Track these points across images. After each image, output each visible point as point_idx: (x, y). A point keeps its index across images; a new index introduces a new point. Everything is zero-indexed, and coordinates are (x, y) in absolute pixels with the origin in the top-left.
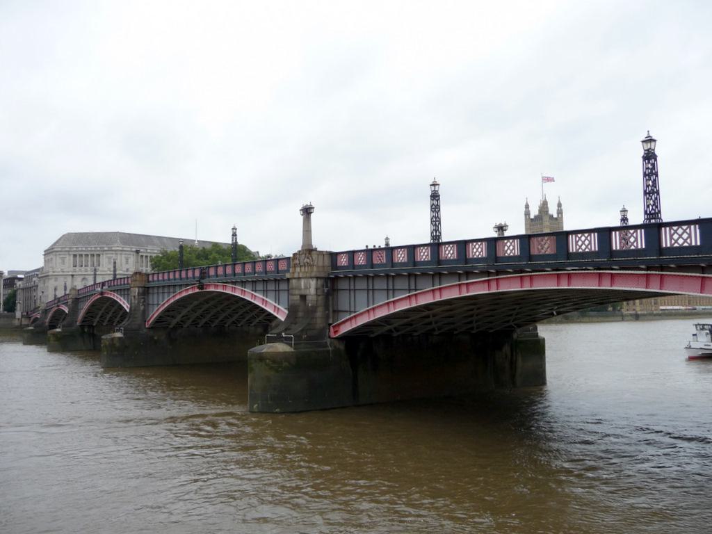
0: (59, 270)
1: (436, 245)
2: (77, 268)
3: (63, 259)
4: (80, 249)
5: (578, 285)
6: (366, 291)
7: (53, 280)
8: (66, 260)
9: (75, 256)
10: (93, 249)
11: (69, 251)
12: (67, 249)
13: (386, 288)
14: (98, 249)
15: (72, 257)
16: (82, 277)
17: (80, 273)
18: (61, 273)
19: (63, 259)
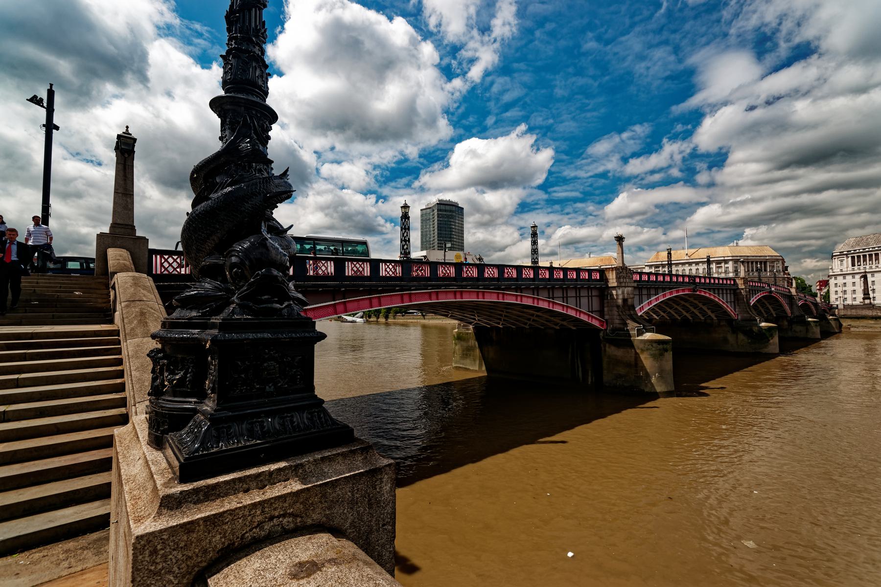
0: (839, 270)
1: (536, 268)
2: (856, 268)
3: (842, 261)
4: (858, 251)
5: (466, 299)
6: (587, 298)
7: (833, 278)
8: (845, 262)
9: (853, 258)
10: (871, 249)
11: (846, 254)
12: (846, 253)
13: (575, 295)
14: (877, 248)
15: (850, 259)
16: (861, 275)
17: (858, 271)
18: (840, 273)
19: (842, 261)
